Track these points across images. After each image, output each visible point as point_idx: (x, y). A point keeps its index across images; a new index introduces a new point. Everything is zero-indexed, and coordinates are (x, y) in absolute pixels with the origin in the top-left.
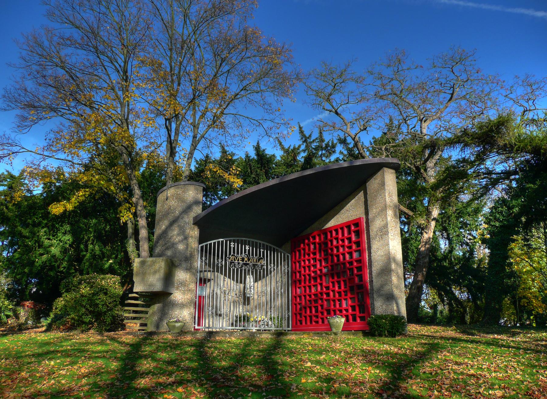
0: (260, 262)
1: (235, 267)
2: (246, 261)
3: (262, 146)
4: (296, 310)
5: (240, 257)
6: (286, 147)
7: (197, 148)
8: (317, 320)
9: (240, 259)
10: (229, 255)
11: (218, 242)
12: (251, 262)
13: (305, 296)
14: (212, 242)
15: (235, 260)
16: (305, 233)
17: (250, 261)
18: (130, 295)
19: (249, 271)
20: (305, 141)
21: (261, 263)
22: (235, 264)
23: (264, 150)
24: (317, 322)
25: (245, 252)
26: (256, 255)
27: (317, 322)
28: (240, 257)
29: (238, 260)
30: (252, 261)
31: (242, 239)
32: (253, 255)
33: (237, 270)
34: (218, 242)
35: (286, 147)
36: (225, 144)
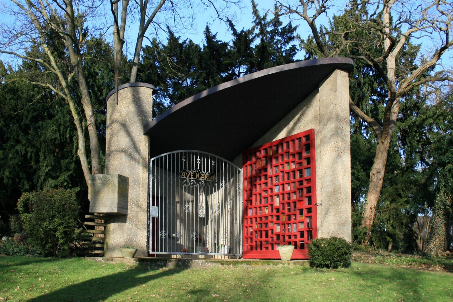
0: (211, 178)
1: (186, 184)
2: (198, 178)
3: (213, 31)
4: (247, 234)
5: (192, 173)
6: (239, 31)
7: (145, 35)
8: (267, 246)
9: (191, 175)
10: (181, 170)
11: (185, 153)
12: (203, 179)
13: (256, 218)
14: (163, 155)
15: (186, 177)
16: (255, 145)
17: (202, 177)
18: (87, 216)
19: (200, 188)
20: (259, 23)
21: (212, 180)
22: (186, 182)
23: (214, 36)
24: (267, 248)
25: (197, 167)
26: (208, 171)
27: (267, 248)
28: (192, 173)
29: (190, 177)
30: (204, 177)
31: (174, 152)
32: (204, 170)
33: (189, 188)
34: (184, 152)
35: (239, 31)
36: (175, 29)
